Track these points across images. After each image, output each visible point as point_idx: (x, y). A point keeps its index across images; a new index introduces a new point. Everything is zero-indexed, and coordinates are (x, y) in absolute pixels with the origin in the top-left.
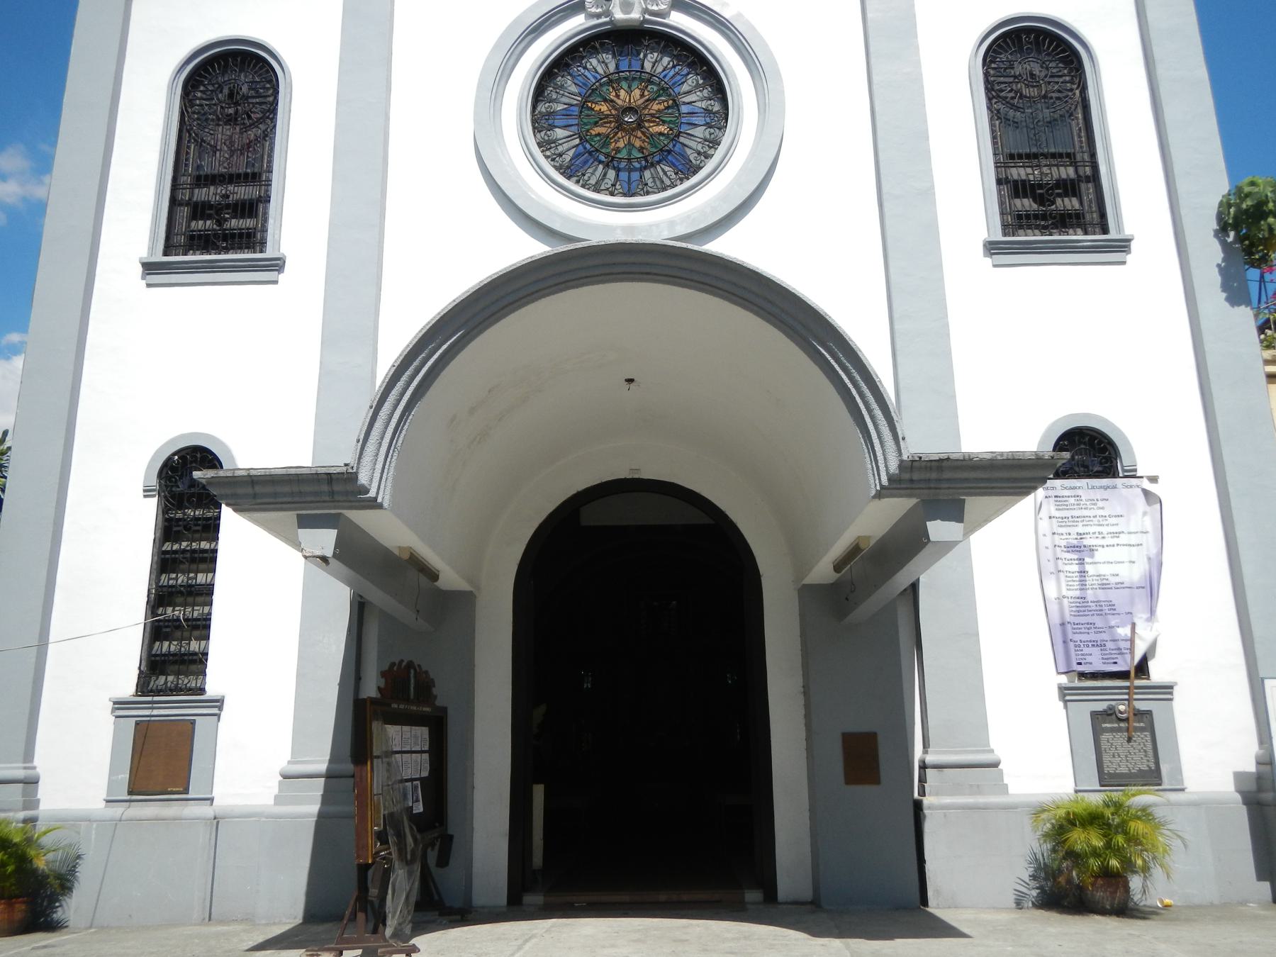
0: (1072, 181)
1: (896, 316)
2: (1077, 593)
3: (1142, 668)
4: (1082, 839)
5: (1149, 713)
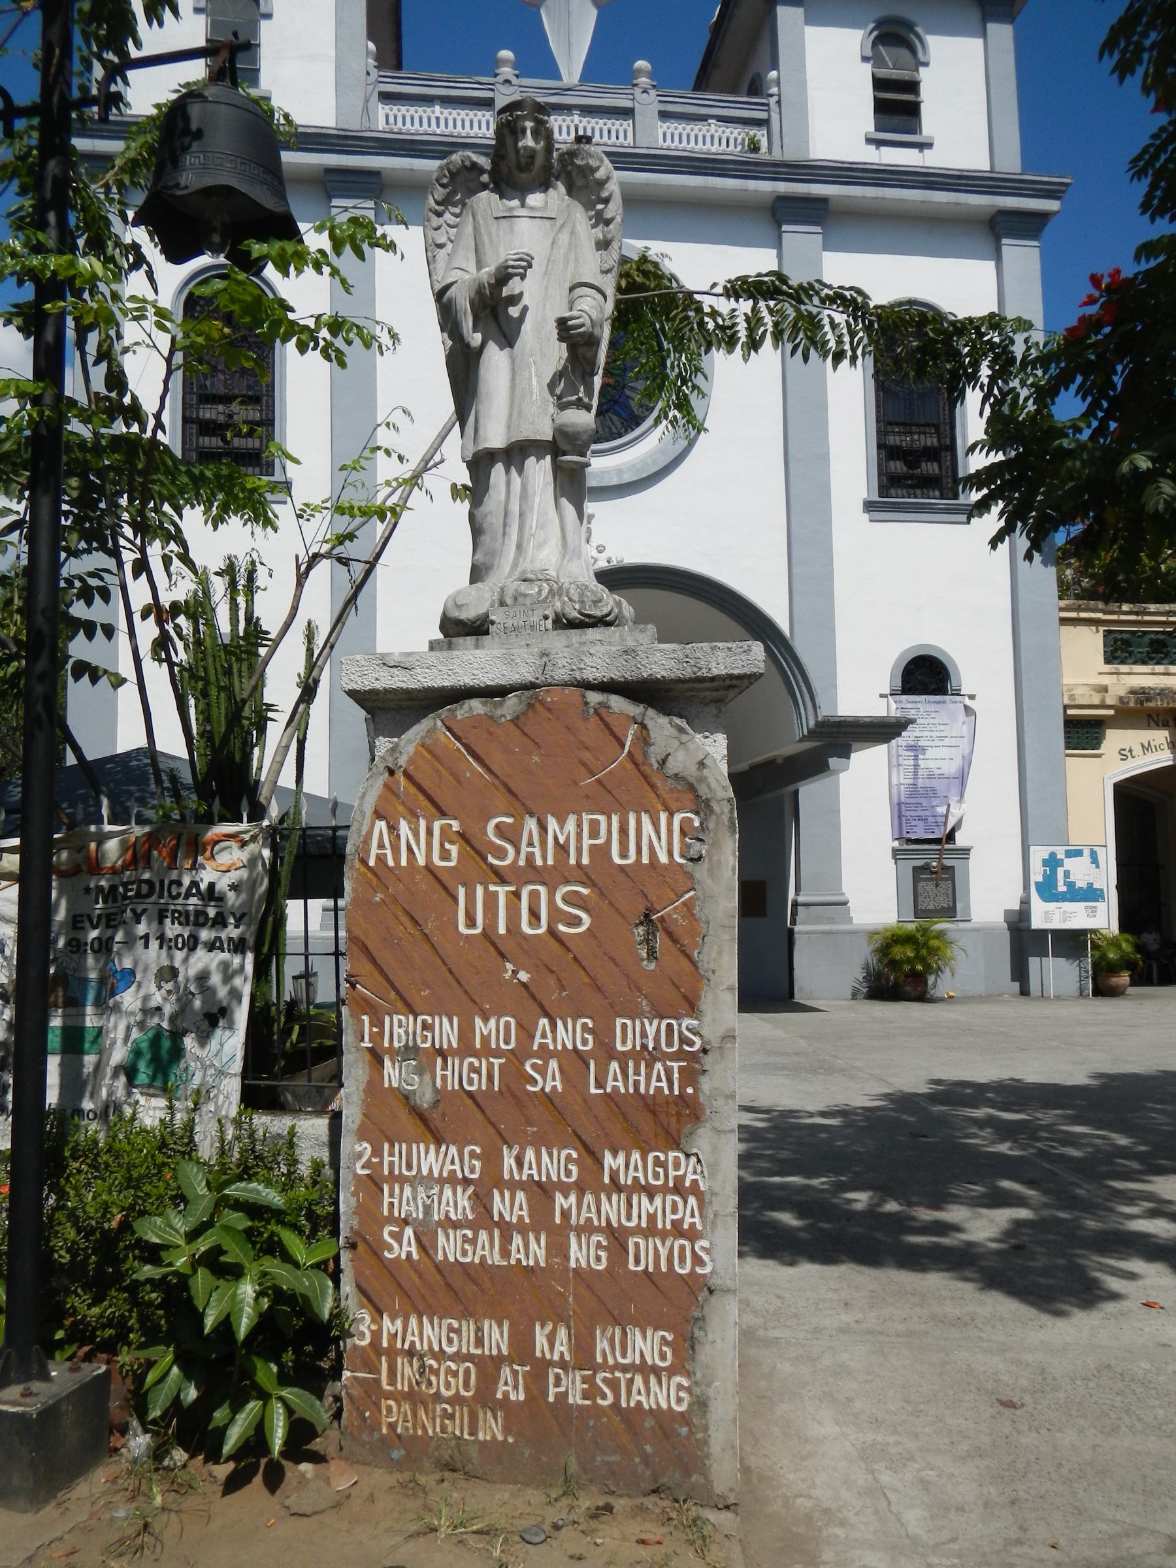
0: (935, 448)
1: (794, 561)
2: (911, 781)
3: (951, 837)
4: (898, 952)
5: (953, 867)
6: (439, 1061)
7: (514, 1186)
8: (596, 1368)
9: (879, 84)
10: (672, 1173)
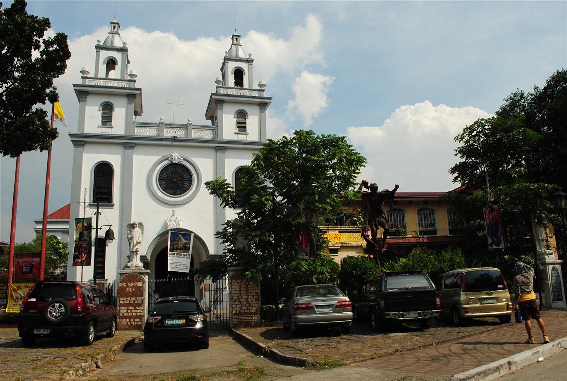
9: (238, 122)
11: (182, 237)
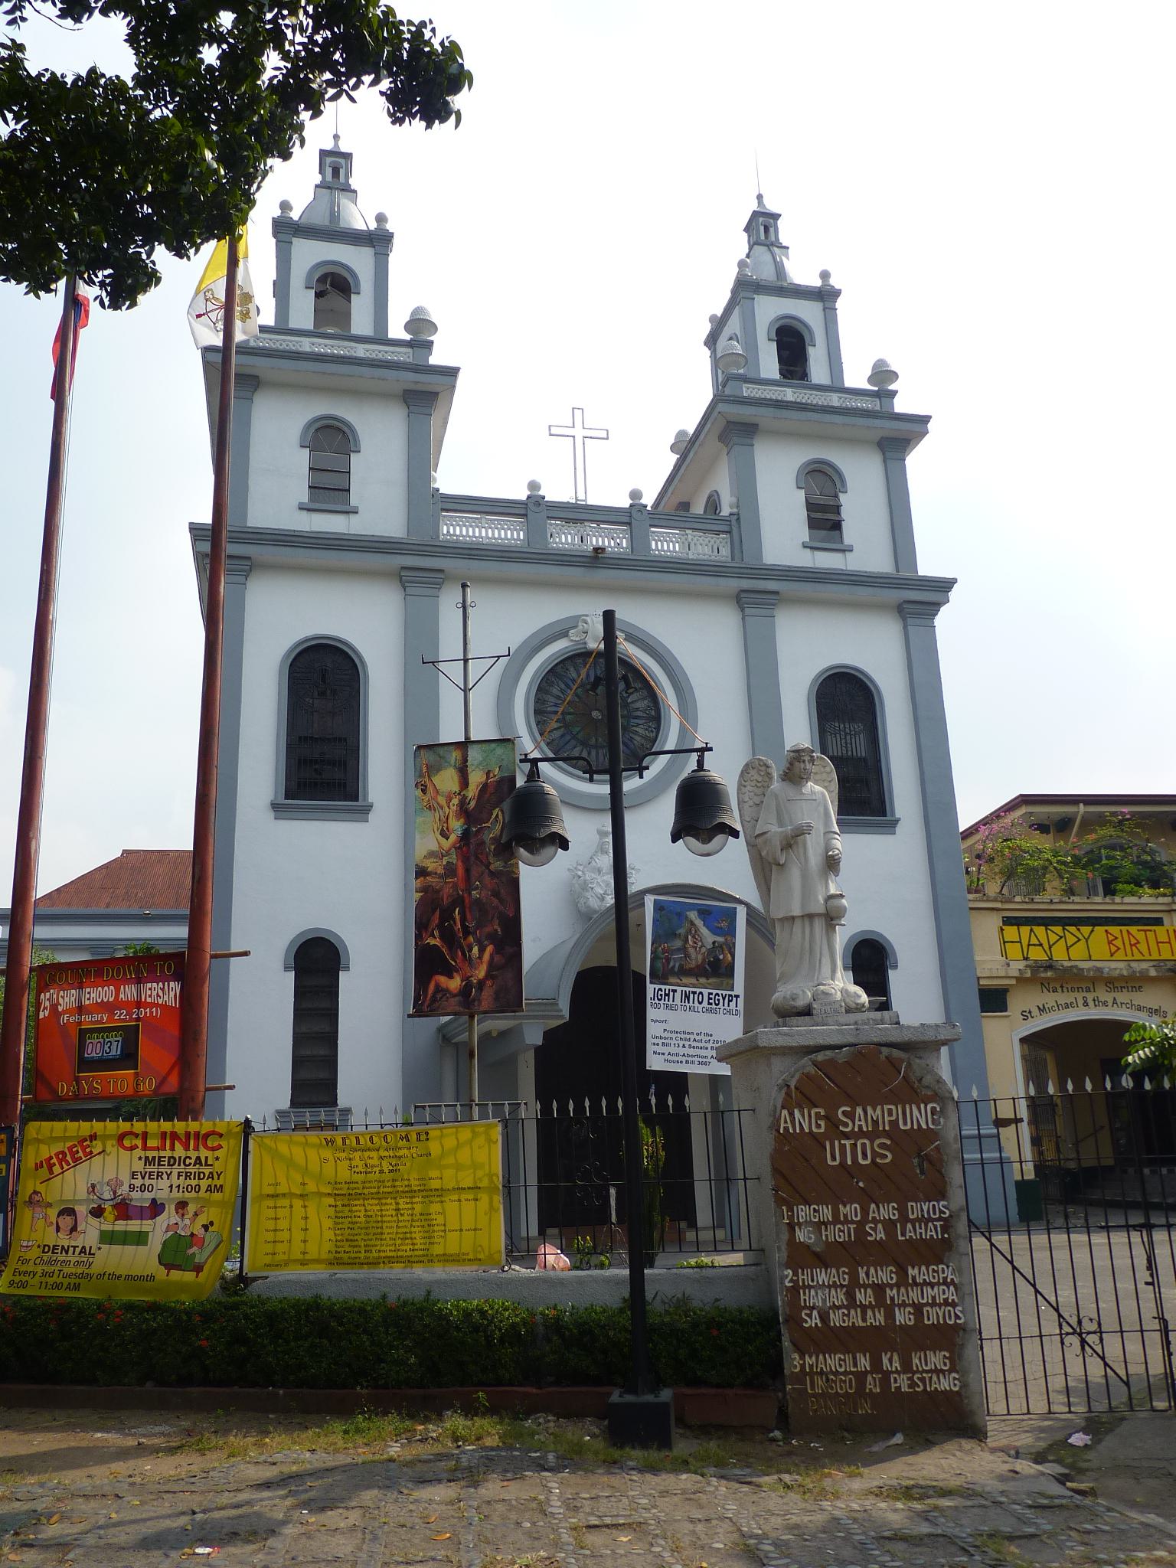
6: (823, 1227)
7: (865, 1286)
8: (914, 1373)
9: (811, 507)
10: (941, 1276)
11: (699, 923)
